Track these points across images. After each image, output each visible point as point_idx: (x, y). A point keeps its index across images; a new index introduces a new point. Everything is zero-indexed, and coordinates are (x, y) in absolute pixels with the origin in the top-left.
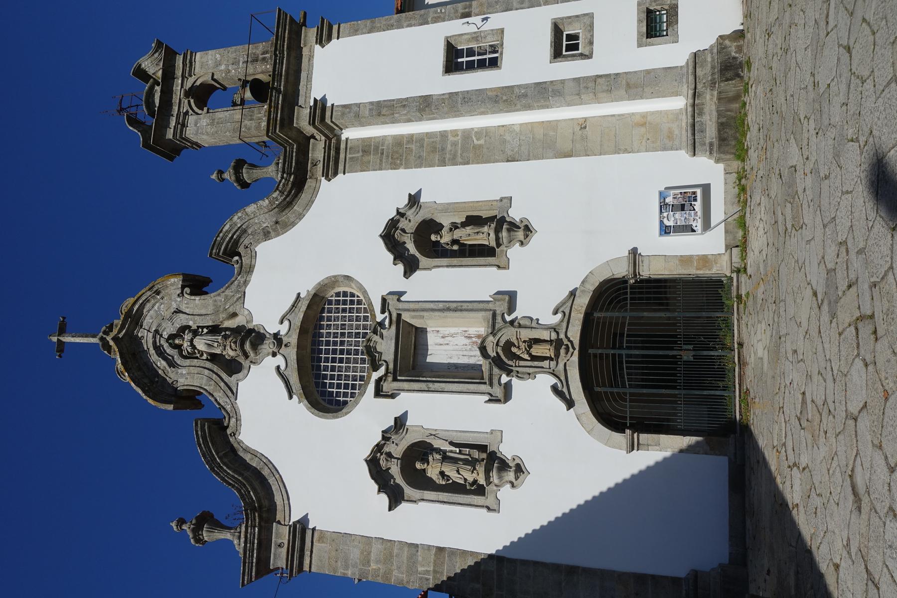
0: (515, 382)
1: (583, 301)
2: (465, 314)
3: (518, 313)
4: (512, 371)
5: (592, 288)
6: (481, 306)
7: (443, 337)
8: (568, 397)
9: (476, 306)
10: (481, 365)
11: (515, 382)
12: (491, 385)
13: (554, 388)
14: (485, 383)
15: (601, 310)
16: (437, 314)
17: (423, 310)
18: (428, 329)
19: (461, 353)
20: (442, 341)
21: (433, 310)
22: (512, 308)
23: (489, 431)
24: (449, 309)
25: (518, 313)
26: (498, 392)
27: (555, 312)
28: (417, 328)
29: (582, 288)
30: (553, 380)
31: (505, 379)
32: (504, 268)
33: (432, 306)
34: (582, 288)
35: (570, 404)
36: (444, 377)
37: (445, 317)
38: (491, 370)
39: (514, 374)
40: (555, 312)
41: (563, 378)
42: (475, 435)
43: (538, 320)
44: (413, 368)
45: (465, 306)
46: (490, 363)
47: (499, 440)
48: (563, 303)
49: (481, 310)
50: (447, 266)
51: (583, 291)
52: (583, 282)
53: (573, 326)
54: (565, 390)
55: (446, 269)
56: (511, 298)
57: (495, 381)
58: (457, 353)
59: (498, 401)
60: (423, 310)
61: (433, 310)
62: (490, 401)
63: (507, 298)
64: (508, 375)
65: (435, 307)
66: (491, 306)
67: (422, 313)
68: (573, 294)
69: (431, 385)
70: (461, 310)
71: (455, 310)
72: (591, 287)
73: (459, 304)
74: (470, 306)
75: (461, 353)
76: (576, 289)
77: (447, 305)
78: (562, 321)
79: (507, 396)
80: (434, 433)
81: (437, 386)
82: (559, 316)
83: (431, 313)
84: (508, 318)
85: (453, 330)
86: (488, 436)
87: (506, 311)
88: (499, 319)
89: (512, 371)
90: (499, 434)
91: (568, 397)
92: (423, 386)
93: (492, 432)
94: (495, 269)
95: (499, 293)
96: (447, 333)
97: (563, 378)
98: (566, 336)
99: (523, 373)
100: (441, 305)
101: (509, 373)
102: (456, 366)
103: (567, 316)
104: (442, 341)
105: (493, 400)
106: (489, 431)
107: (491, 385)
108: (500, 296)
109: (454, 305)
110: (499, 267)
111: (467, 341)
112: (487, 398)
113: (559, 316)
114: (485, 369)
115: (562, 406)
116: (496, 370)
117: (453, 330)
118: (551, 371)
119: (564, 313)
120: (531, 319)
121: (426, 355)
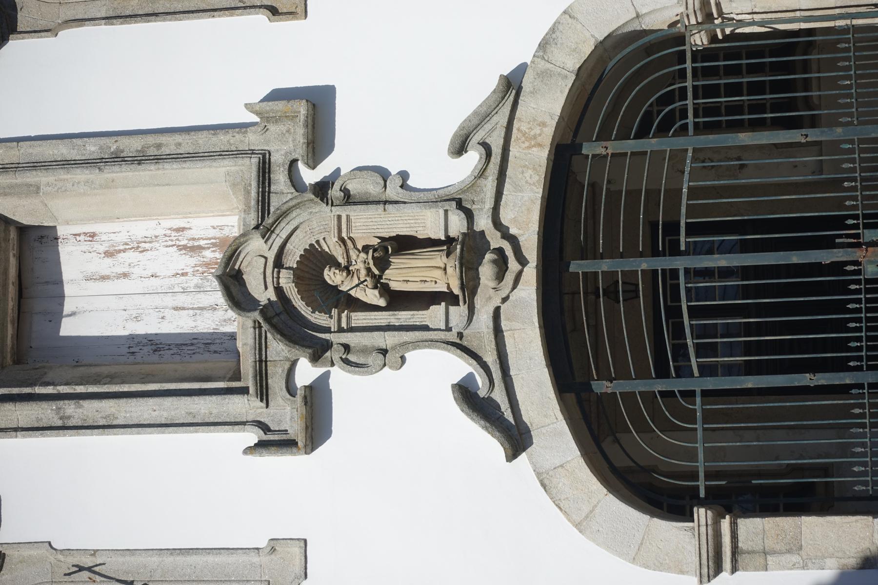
0: (341, 380)
1: (544, 109)
2: (171, 170)
3: (342, 159)
4: (327, 346)
5: (573, 63)
6: (222, 141)
7: (109, 254)
8: (509, 416)
9: (204, 142)
10: (232, 337)
11: (341, 380)
12: (264, 394)
13: (466, 394)
14: (244, 391)
15: (604, 136)
16: (81, 175)
17: (36, 166)
18: (61, 231)
19: (169, 301)
20: (105, 266)
21: (66, 164)
22: (319, 143)
23: (263, 543)
24: (118, 159)
25: (342, 159)
26: (286, 415)
27: (460, 148)
28: (23, 230)
29: (542, 65)
30: (460, 367)
31: (306, 373)
32: (292, 14)
33: (63, 150)
34: (542, 65)
35: (516, 439)
36: (112, 379)
37: (108, 186)
38: (261, 346)
39: (335, 354)
40: (460, 148)
41: (491, 358)
42: (211, 559)
43: (404, 175)
44: (18, 360)
45: (170, 144)
46: (257, 326)
47: (298, 569)
48: (482, 117)
49: (222, 154)
50: (109, 19)
51: (544, 75)
52: (543, 45)
53: (518, 188)
54: (499, 396)
55: (104, 29)
56: (317, 111)
57: (276, 383)
58: (157, 300)
59: (287, 444)
60: (36, 166)
61: (66, 164)
62: (262, 445)
63: (302, 108)
64: (315, 359)
65: (74, 155)
66: (253, 140)
67: (31, 177)
68: (512, 85)
69: (69, 408)
70: (157, 159)
71: (140, 159)
72: (571, 59)
73: (151, 140)
74: (187, 144)
75: (169, 301)
76: (522, 69)
77: (113, 145)
78: (482, 173)
79: (316, 427)
80: (88, 562)
81: (91, 410)
82: (473, 158)
83: (62, 174)
84: (310, 176)
85: (140, 229)
86: (264, 559)
87: (299, 152)
88: (280, 178)
89: (327, 346)
90: (297, 550)
91: (509, 416)
92: (45, 412)
93: (274, 546)
94: (261, 18)
95: (276, 95)
96: (122, 237)
97: (491, 358)
98: (497, 223)
99: (365, 351)
100: (92, 148)
101: (318, 351)
102: (156, 344)
103: (496, 159)
104: (105, 266)
105: (273, 442)
106: (263, 543)
107: (264, 394)
108: (280, 106)
109: (133, 145)
110: (274, 11)
111: (187, 262)
112: (252, 437)
113: (473, 158)
114: (245, 344)
115: (491, 446)
116: (277, 348)
117: (140, 229)
118: (452, 337)
119: (486, 147)
120: (383, 174)
121: (56, 315)
